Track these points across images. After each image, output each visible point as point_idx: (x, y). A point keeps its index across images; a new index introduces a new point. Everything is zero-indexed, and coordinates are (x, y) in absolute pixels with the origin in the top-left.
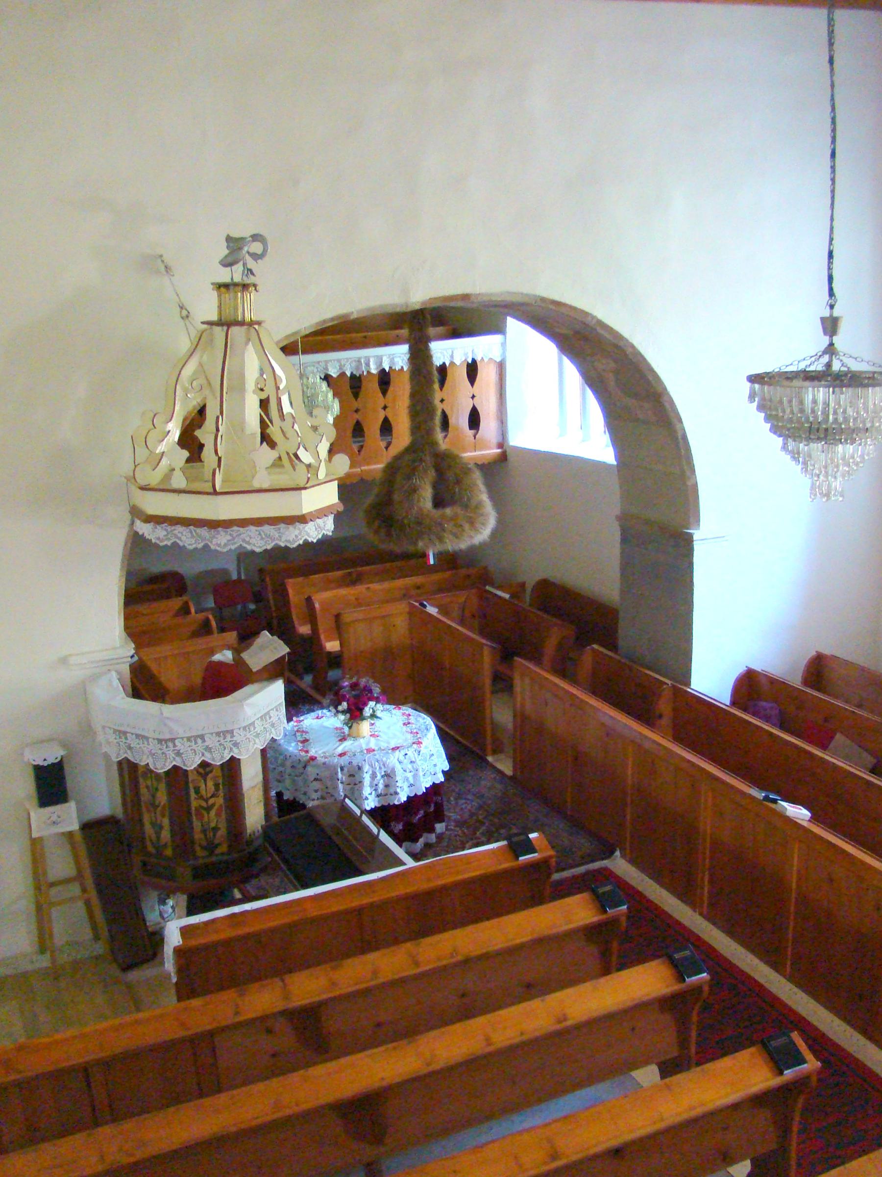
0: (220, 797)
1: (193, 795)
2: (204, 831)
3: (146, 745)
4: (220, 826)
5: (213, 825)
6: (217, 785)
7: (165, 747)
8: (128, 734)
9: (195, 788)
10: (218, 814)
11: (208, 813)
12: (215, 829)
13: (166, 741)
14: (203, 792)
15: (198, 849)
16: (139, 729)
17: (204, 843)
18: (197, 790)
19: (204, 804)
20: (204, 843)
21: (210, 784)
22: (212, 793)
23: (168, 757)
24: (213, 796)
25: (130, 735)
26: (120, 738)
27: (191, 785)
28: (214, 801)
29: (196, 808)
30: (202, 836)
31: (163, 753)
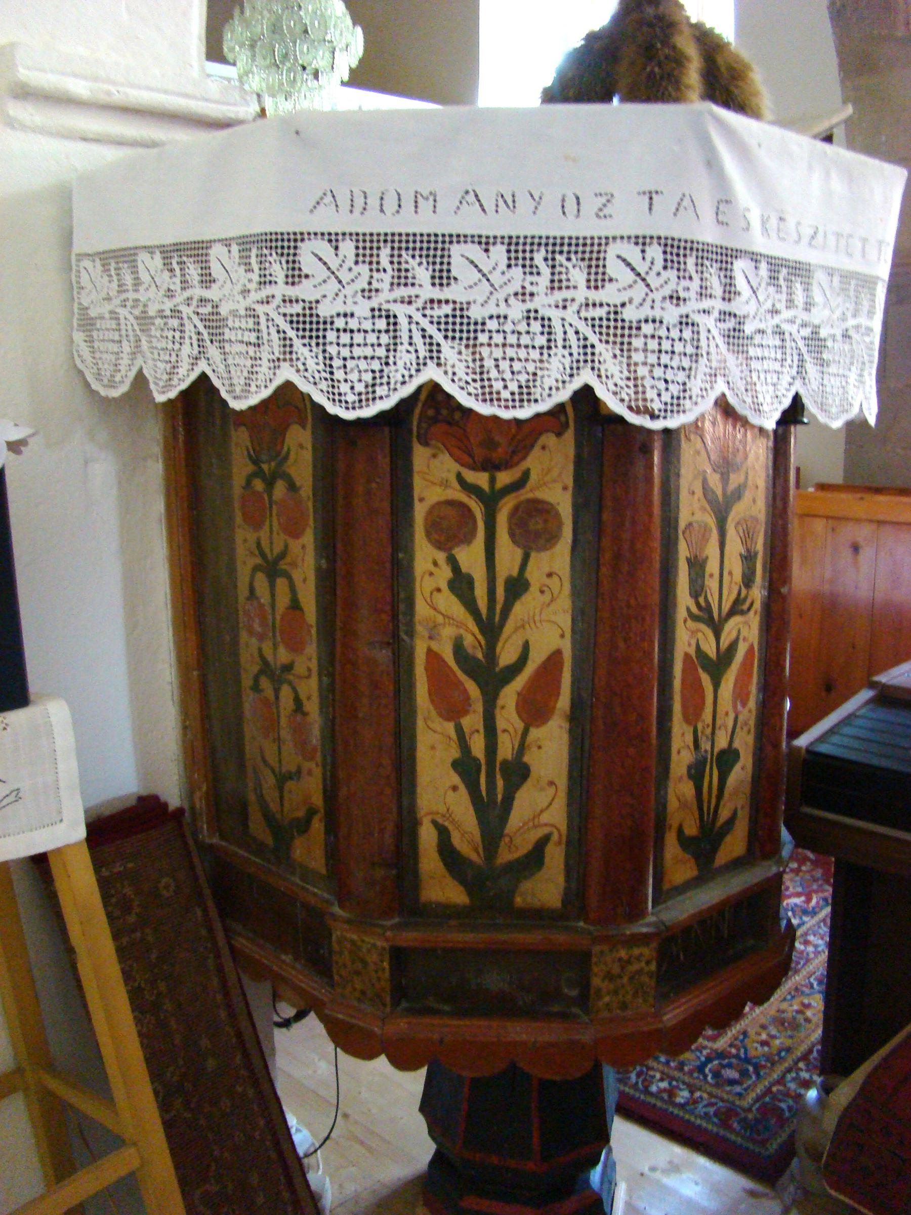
0: (752, 613)
1: (684, 600)
2: (696, 773)
3: (582, 294)
4: (736, 744)
5: (722, 742)
6: (748, 558)
7: (695, 285)
8: (456, 250)
9: (689, 560)
10: (740, 695)
11: (716, 685)
12: (727, 758)
13: (702, 252)
14: (712, 584)
15: (672, 848)
16: (537, 201)
17: (691, 830)
18: (697, 565)
19: (710, 649)
20: (691, 830)
21: (734, 546)
22: (734, 595)
23: (703, 343)
24: (737, 608)
25: (474, 251)
26: (402, 278)
27: (683, 551)
28: (734, 635)
29: (687, 656)
30: (687, 789)
31: (685, 322)
